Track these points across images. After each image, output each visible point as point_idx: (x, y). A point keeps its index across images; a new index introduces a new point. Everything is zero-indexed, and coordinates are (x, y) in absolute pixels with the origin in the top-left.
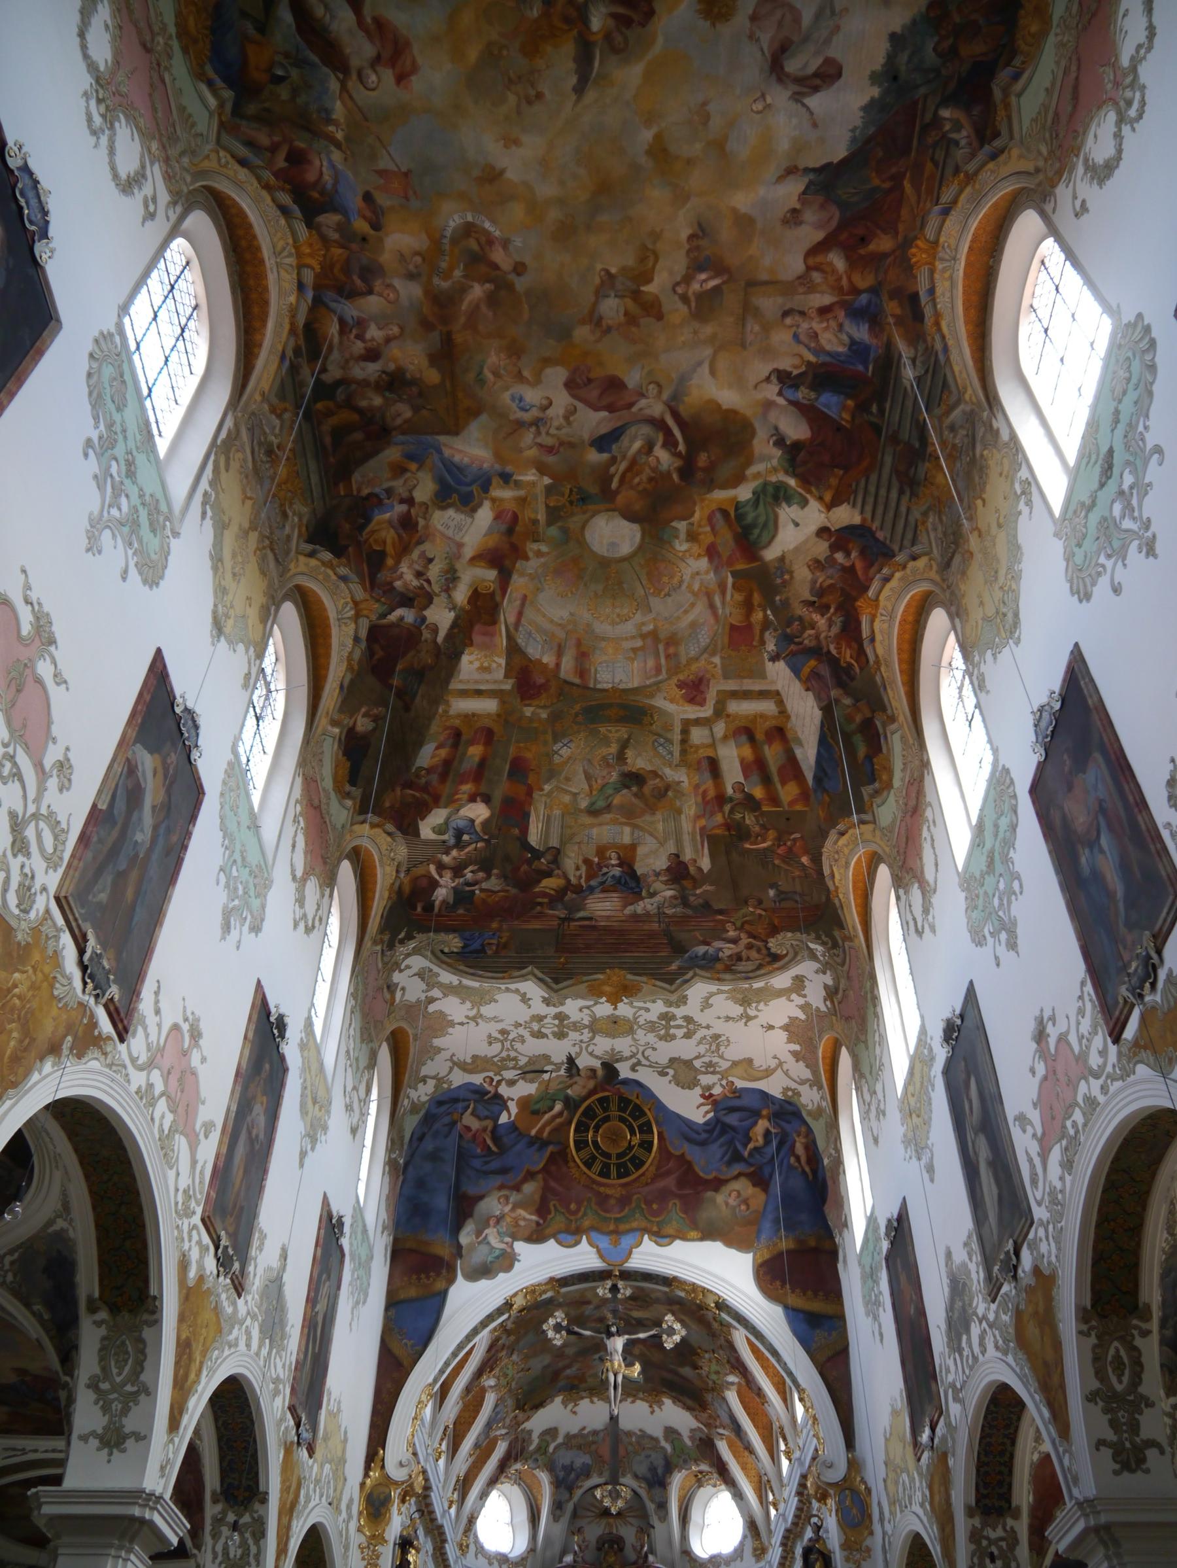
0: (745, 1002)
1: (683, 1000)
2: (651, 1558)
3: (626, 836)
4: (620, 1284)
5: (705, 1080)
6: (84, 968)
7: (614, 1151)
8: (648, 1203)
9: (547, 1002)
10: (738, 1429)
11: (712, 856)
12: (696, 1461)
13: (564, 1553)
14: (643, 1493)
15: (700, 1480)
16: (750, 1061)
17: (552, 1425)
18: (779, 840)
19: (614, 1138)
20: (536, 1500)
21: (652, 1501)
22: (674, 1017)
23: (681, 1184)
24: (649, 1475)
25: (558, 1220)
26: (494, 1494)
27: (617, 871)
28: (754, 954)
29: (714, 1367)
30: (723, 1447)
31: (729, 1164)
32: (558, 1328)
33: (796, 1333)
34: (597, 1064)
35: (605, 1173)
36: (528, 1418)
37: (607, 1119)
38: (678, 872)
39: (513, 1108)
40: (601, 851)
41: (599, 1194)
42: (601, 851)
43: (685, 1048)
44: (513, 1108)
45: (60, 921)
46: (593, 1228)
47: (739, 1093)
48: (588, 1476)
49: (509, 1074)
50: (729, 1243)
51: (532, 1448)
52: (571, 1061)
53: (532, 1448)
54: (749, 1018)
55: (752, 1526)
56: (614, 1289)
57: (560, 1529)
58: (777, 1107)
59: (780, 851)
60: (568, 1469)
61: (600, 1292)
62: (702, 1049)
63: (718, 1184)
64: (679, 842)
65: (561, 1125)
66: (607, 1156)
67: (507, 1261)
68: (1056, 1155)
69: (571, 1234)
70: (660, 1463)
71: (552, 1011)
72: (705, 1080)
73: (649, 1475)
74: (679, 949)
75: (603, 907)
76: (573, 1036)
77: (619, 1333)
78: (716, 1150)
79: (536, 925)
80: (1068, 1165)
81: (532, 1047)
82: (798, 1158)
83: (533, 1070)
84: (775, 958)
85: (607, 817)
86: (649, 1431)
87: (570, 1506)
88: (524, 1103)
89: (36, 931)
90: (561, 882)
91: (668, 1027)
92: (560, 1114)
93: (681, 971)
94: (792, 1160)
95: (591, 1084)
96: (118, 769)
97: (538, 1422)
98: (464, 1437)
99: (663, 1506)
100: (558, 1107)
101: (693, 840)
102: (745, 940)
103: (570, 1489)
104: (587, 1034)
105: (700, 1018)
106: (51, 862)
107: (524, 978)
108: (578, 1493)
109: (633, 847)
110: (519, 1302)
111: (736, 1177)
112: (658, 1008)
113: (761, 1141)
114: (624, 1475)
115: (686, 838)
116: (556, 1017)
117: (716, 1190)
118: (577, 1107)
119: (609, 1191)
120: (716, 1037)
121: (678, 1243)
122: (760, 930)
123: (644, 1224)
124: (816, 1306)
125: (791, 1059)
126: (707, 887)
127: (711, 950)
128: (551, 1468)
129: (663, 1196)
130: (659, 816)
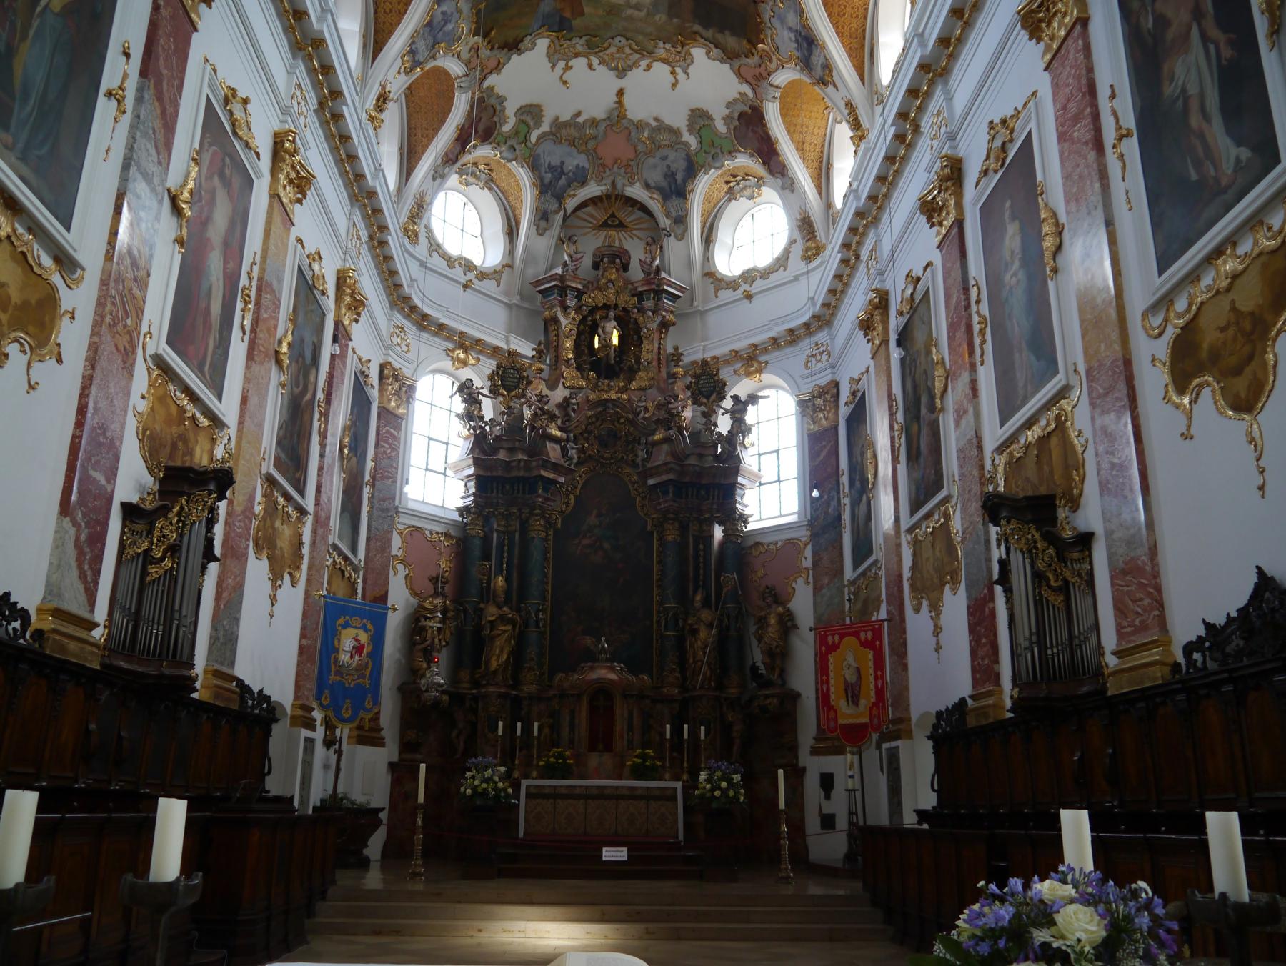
2: (663, 275)
10: (808, 41)
12: (731, 153)
13: (552, 268)
14: (655, 205)
15: (734, 187)
17: (535, 102)
20: (513, 211)
21: (668, 216)
24: (664, 184)
36: (498, 67)
48: (583, 183)
51: (506, 128)
53: (506, 128)
55: (805, 226)
57: (544, 245)
60: (558, 171)
70: (680, 166)
73: (664, 184)
86: (667, 122)
98: (390, 33)
99: (681, 221)
103: (560, 198)
114: (631, 184)
128: (533, 164)
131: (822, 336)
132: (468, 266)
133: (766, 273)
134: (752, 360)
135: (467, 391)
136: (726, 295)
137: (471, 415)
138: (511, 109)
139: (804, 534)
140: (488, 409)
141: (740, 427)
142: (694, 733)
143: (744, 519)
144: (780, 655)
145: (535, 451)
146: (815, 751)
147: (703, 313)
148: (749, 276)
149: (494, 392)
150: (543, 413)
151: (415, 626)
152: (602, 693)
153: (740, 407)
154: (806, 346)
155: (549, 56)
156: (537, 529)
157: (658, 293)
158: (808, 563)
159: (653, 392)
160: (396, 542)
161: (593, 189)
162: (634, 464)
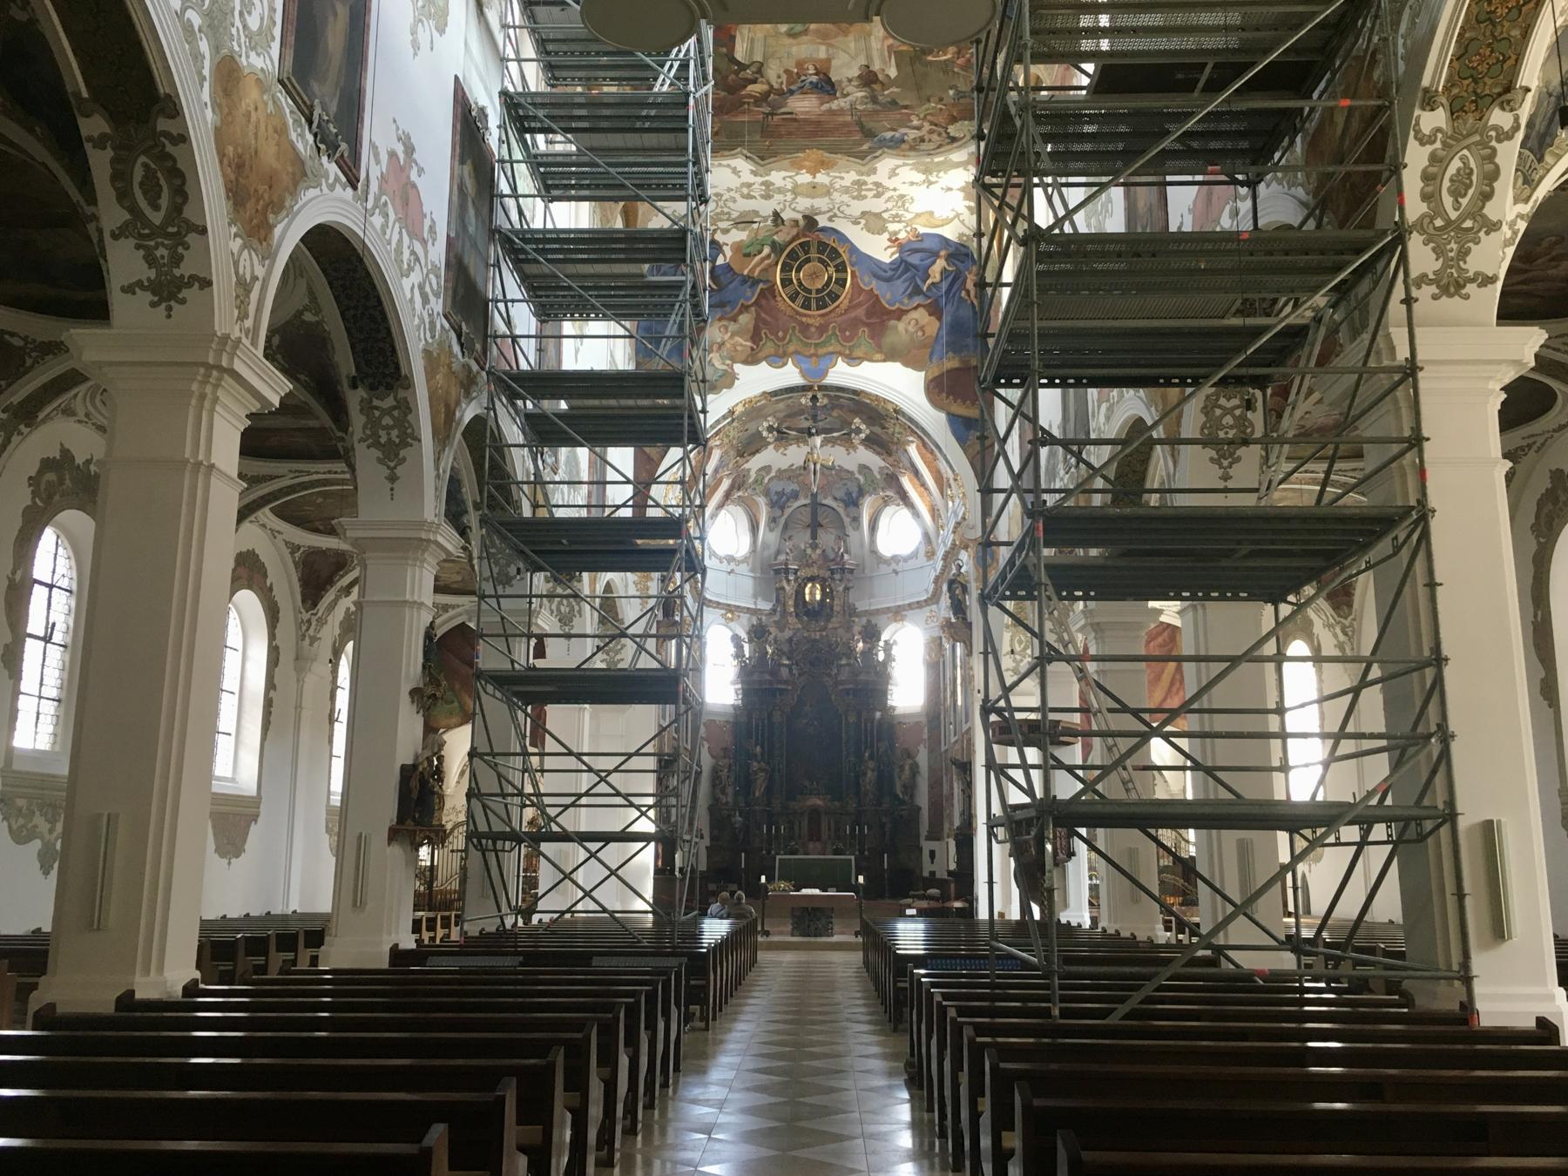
0: (927, 171)
1: (874, 171)
2: (846, 557)
3: (822, 53)
4: (819, 395)
5: (892, 227)
6: (462, 346)
7: (813, 288)
8: (843, 331)
9: (755, 173)
11: (898, 66)
14: (841, 510)
15: (886, 502)
16: (931, 213)
18: (959, 53)
19: (814, 276)
22: (865, 183)
23: (869, 314)
25: (769, 348)
26: (723, 512)
27: (814, 79)
28: (935, 137)
29: (897, 429)
30: (906, 482)
31: (910, 296)
32: (770, 429)
33: (955, 433)
34: (799, 217)
35: (806, 306)
37: (808, 260)
38: (869, 78)
39: (728, 252)
40: (800, 64)
41: (801, 324)
42: (800, 64)
43: (876, 205)
44: (727, 250)
45: (447, 325)
46: (797, 352)
47: (922, 237)
49: (723, 225)
50: (906, 364)
52: (776, 215)
54: (931, 183)
55: (927, 537)
56: (814, 398)
58: (951, 250)
59: (960, 61)
60: (781, 494)
61: (803, 401)
62: (890, 205)
63: (900, 314)
64: (869, 57)
65: (770, 265)
66: (809, 292)
67: (728, 380)
68: (1104, 406)
69: (778, 359)
71: (759, 179)
72: (892, 227)
74: (869, 134)
75: (804, 105)
76: (778, 197)
77: (818, 433)
78: (900, 285)
79: (746, 118)
80: (1108, 418)
81: (744, 205)
82: (968, 292)
83: (744, 221)
84: (954, 140)
85: (805, 38)
87: (782, 521)
88: (737, 247)
89: (440, 344)
90: (765, 87)
91: (860, 190)
92: (768, 256)
93: (872, 150)
94: (963, 294)
95: (794, 232)
96: (455, 198)
97: (755, 463)
99: (856, 520)
100: (767, 250)
101: (882, 55)
102: (927, 126)
103: (782, 508)
104: (789, 196)
105: (886, 183)
106: (437, 295)
107: (734, 156)
108: (788, 511)
109: (829, 61)
110: (740, 409)
111: (915, 308)
112: (851, 177)
113: (938, 278)
115: (875, 54)
116: (763, 184)
117: (899, 319)
118: (782, 251)
119: (810, 321)
120: (902, 197)
121: (865, 364)
122: (941, 120)
123: (839, 348)
124: (973, 413)
125: (966, 212)
126: (894, 89)
127: (897, 135)
128: (767, 493)
129: (855, 324)
130: (851, 37)
131: (934, 607)
132: (730, 559)
133: (906, 559)
134: (898, 613)
135: (736, 640)
136: (884, 569)
137: (739, 655)
138: (753, 475)
139: (924, 720)
140: (746, 647)
141: (889, 657)
142: (861, 830)
143: (894, 708)
144: (911, 788)
145: (774, 673)
146: (928, 838)
147: (871, 578)
148: (895, 559)
149: (750, 641)
150: (779, 652)
151: (715, 771)
152: (815, 813)
153: (888, 647)
154: (926, 611)
155: (776, 448)
156: (777, 717)
157: (843, 570)
158: (925, 736)
159: (841, 631)
160: (702, 730)
161: (802, 501)
162: (829, 675)
